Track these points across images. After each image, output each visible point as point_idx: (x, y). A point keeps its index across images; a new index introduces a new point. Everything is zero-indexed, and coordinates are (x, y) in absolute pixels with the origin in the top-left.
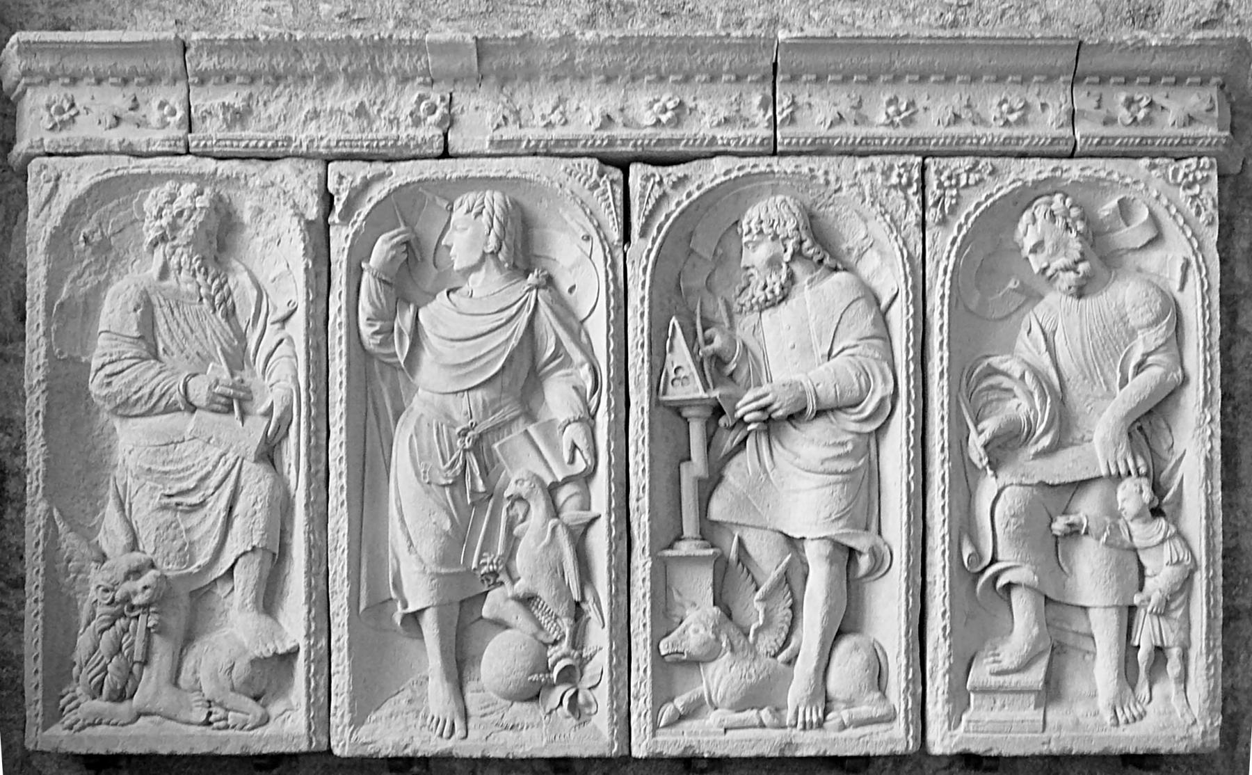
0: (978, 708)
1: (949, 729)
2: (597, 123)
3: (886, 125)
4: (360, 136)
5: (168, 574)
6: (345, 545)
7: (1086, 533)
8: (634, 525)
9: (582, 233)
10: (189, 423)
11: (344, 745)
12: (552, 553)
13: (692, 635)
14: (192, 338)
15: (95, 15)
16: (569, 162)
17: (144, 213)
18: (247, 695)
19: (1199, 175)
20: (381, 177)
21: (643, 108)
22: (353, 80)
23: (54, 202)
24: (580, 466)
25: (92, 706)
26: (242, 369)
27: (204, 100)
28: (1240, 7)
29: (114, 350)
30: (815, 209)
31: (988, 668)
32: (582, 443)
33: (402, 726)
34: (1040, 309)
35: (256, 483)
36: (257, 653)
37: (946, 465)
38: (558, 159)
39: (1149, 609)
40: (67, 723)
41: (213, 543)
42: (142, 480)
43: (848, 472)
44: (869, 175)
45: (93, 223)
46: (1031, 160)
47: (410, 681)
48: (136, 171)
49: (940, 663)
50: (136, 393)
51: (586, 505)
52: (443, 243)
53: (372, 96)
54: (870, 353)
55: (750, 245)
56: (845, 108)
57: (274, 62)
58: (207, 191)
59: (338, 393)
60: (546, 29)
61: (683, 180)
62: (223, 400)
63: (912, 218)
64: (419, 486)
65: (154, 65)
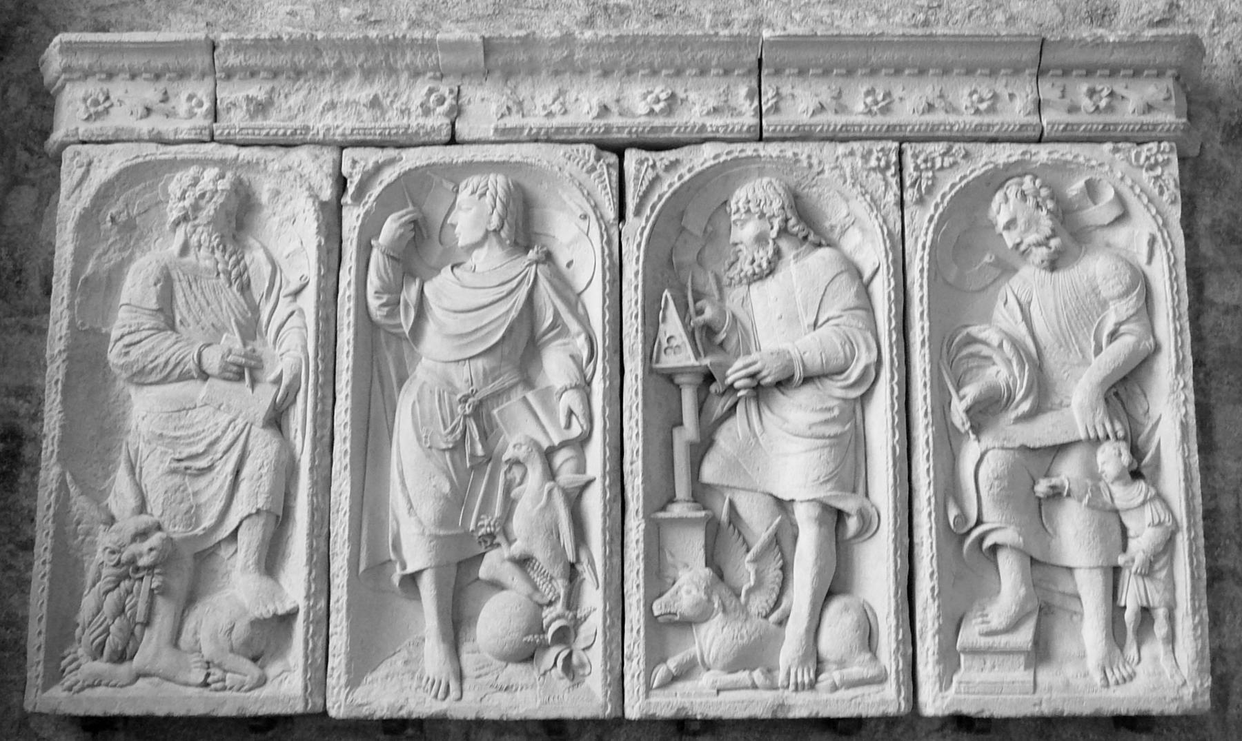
0: (969, 668)
1: (941, 690)
2: (595, 112)
5: (174, 536)
6: (347, 508)
7: (1069, 495)
8: (628, 488)
9: (580, 213)
11: (339, 707)
12: (548, 516)
14: (208, 310)
16: (568, 148)
17: (168, 195)
18: (245, 656)
19: (1160, 158)
20: (391, 162)
21: (638, 99)
22: (368, 75)
23: (85, 185)
24: (576, 430)
26: (254, 339)
27: (228, 93)
28: (1190, 7)
29: (134, 322)
30: (799, 190)
31: (977, 629)
32: (578, 409)
33: (398, 687)
35: (264, 448)
36: (257, 614)
37: (930, 430)
38: (557, 145)
39: (1133, 570)
40: (67, 684)
41: (218, 506)
42: (154, 445)
43: (835, 436)
44: (850, 159)
45: (120, 204)
46: (1002, 145)
47: (406, 642)
48: (163, 157)
49: (930, 624)
50: (152, 362)
51: (581, 468)
52: (448, 222)
53: (386, 89)
54: (854, 323)
56: (826, 97)
57: (296, 59)
58: (229, 175)
59: (345, 362)
60: (548, 29)
61: (674, 165)
62: (235, 369)
63: (891, 198)
65: (184, 62)
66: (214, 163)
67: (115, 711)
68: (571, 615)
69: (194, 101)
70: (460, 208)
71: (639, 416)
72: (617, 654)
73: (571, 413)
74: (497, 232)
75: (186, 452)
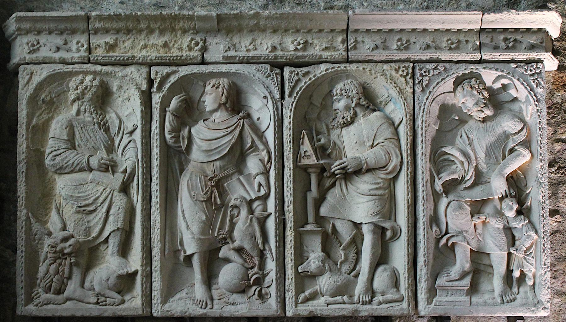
0: (441, 295)
2: (269, 50)
3: (397, 50)
4: (165, 55)
9: (263, 95)
10: (90, 176)
12: (250, 229)
13: (313, 264)
14: (91, 140)
15: (45, 5)
16: (258, 66)
17: (69, 88)
20: (174, 72)
21: (290, 43)
22: (162, 32)
24: (263, 192)
25: (45, 296)
26: (112, 153)
27: (95, 40)
29: (57, 145)
30: (365, 85)
32: (263, 183)
33: (184, 304)
34: (466, 127)
35: (119, 201)
36: (119, 273)
40: (35, 303)
42: (68, 201)
43: (382, 195)
45: (47, 92)
48: (66, 70)
49: (423, 276)
50: (66, 163)
51: (265, 209)
53: (170, 39)
55: (337, 100)
56: (378, 42)
57: (128, 25)
58: (98, 78)
61: (307, 73)
62: (105, 166)
64: (191, 201)
65: (74, 26)
66: (90, 73)
67: (58, 314)
68: (261, 273)
69: (80, 45)
70: (207, 94)
71: (291, 186)
72: (282, 289)
73: (260, 185)
74: (224, 104)
75: (84, 203)
